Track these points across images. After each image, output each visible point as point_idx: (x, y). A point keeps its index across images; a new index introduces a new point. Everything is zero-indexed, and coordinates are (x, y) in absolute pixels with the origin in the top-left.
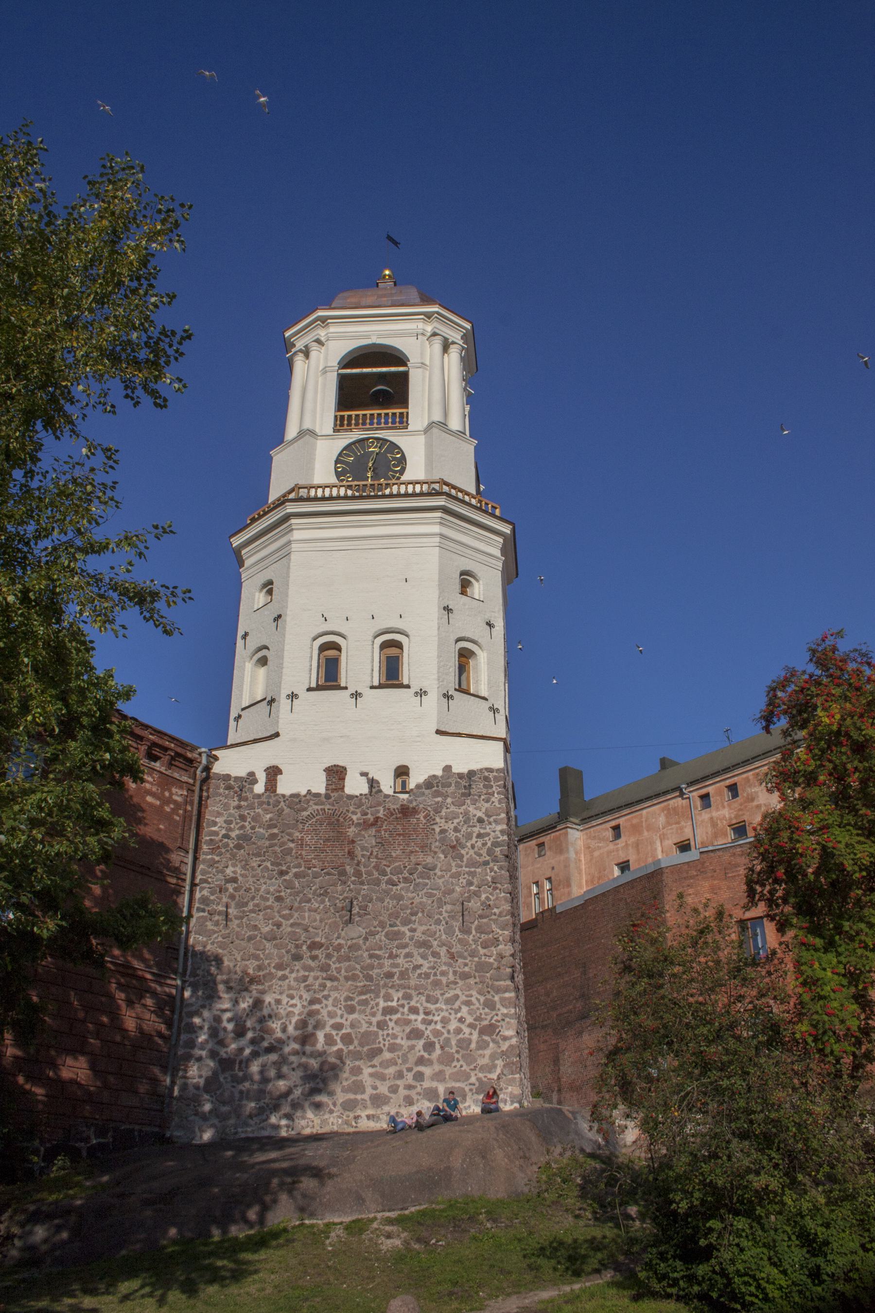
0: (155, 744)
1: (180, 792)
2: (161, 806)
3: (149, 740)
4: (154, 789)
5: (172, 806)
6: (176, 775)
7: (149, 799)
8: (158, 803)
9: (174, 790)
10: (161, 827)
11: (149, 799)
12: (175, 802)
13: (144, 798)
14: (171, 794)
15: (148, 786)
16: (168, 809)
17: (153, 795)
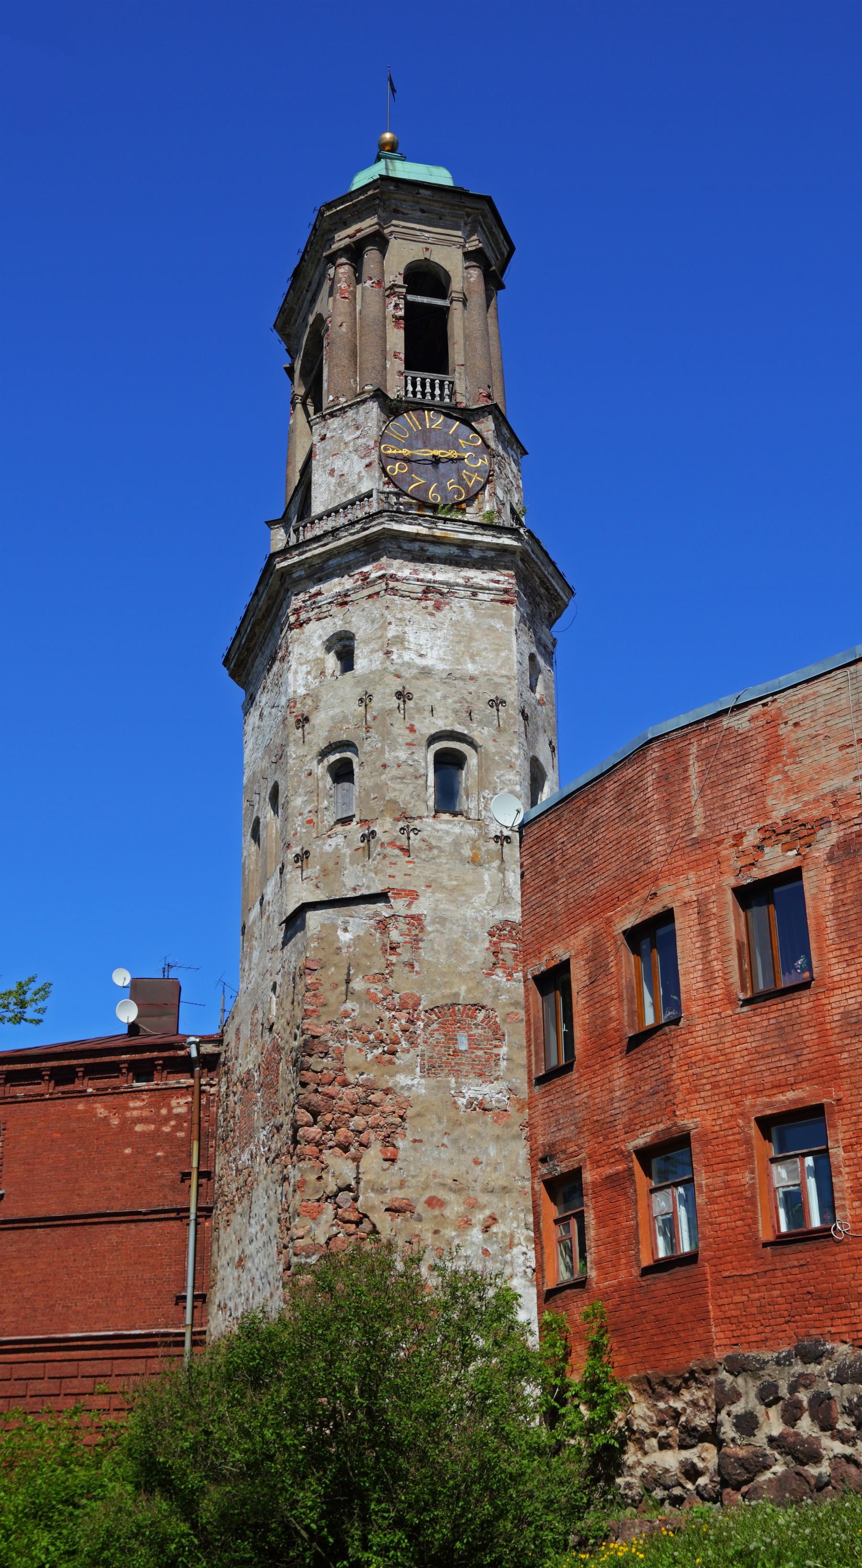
1: (182, 1101)
2: (158, 1130)
3: (124, 1062)
4: (146, 1113)
5: (173, 1123)
6: (172, 1083)
7: (139, 1128)
8: (152, 1127)
9: (174, 1102)
10: (159, 1154)
11: (139, 1128)
12: (178, 1116)
13: (132, 1129)
14: (170, 1109)
15: (135, 1113)
16: (167, 1129)
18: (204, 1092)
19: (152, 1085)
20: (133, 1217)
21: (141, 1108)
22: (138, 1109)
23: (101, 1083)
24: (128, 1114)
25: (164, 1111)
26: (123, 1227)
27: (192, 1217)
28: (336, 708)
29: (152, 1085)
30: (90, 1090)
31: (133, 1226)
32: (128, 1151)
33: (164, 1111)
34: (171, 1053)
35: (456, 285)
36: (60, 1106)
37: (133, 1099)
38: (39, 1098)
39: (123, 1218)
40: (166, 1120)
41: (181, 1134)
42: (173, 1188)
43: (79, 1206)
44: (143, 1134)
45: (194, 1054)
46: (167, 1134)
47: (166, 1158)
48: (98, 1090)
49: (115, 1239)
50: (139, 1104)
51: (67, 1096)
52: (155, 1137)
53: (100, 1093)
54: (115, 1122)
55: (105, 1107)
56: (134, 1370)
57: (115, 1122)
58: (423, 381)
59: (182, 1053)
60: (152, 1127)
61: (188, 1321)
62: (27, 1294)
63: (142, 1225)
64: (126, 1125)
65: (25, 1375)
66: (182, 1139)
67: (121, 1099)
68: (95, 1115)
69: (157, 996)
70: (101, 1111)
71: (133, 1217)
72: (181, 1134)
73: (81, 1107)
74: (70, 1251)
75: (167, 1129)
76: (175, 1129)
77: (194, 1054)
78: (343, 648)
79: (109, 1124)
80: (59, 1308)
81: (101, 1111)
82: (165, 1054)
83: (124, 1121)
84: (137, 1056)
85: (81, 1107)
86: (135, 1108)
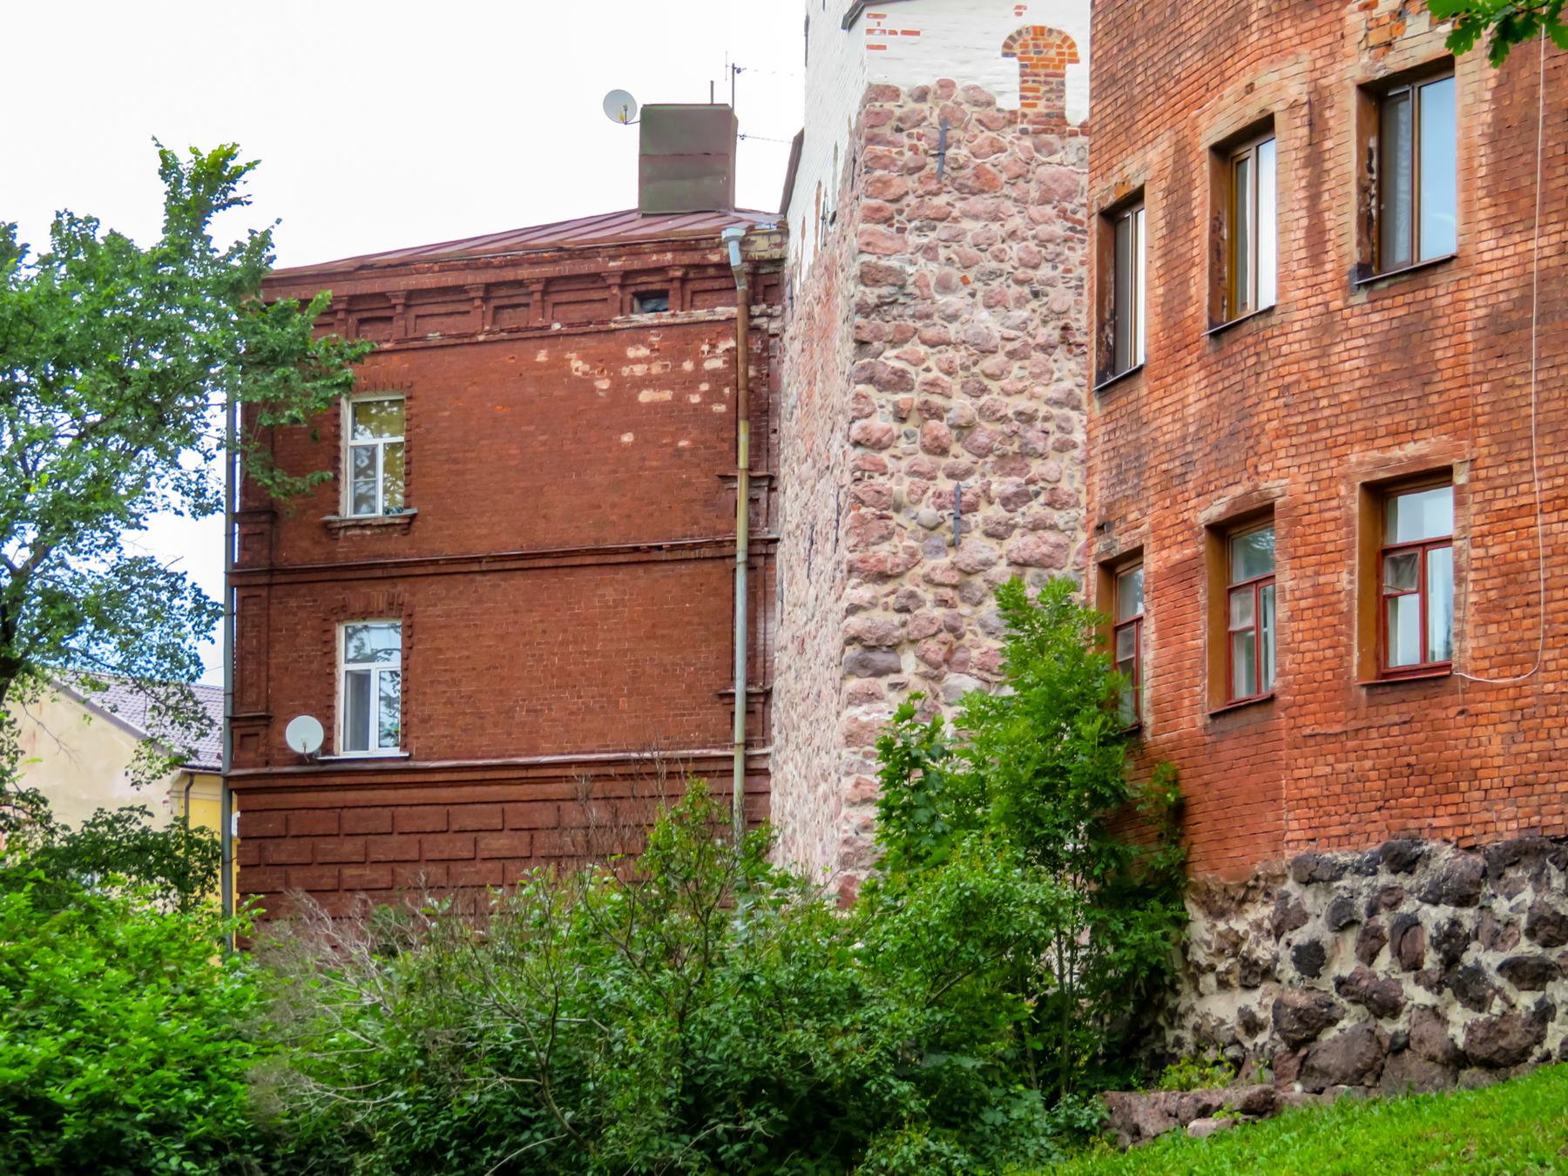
2: (678, 398)
3: (612, 273)
4: (656, 369)
5: (704, 387)
6: (701, 314)
7: (645, 396)
8: (667, 395)
10: (683, 443)
11: (645, 396)
12: (714, 375)
13: (633, 399)
15: (639, 370)
16: (695, 399)
18: (757, 329)
19: (666, 318)
22: (641, 361)
23: (576, 314)
24: (626, 371)
25: (688, 366)
26: (622, 574)
27: (741, 557)
29: (666, 318)
30: (556, 326)
31: (640, 571)
32: (627, 438)
33: (688, 366)
34: (695, 257)
36: (506, 357)
38: (464, 341)
40: (691, 382)
41: (720, 408)
43: (547, 536)
44: (652, 406)
46: (695, 407)
47: (693, 450)
48: (571, 325)
50: (644, 352)
51: (518, 335)
53: (576, 332)
54: (603, 384)
55: (584, 359)
57: (603, 384)
60: (667, 395)
61: (739, 737)
62: (466, 688)
63: (657, 571)
64: (624, 390)
65: (470, 824)
66: (721, 416)
67: (610, 344)
68: (568, 373)
71: (641, 557)
72: (720, 408)
73: (542, 357)
74: (536, 616)
76: (709, 398)
77: (735, 260)
79: (593, 390)
80: (521, 715)
81: (578, 366)
83: (618, 383)
85: (542, 357)
86: (638, 361)
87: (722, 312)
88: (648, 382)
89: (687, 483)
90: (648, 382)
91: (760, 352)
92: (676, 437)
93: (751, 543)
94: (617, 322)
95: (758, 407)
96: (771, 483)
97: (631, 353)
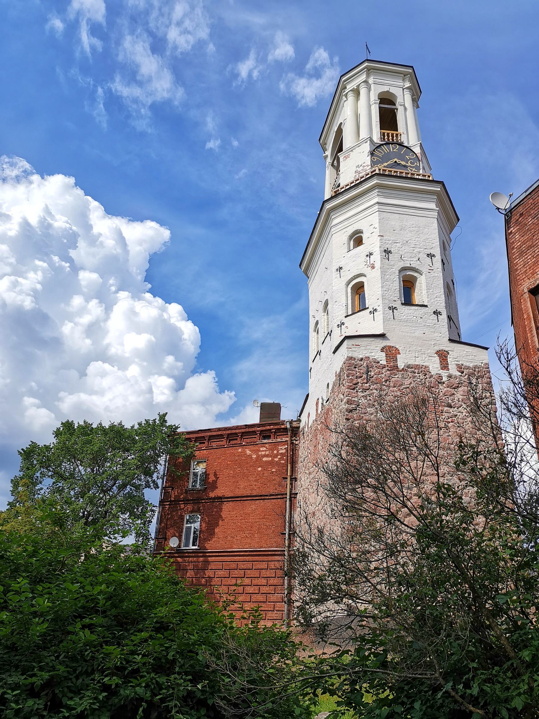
0: (262, 431)
5: (279, 457)
6: (279, 440)
7: (265, 459)
11: (265, 459)
15: (263, 453)
16: (276, 459)
17: (267, 456)
19: (270, 441)
20: (262, 497)
21: (266, 451)
23: (248, 440)
24: (260, 453)
25: (275, 452)
27: (288, 497)
28: (354, 262)
29: (270, 441)
31: (262, 501)
32: (260, 469)
33: (275, 452)
34: (278, 427)
35: (399, 100)
37: (262, 447)
39: (257, 498)
40: (276, 456)
42: (280, 485)
43: (238, 493)
44: (266, 462)
45: (288, 426)
48: (247, 443)
49: (254, 507)
50: (265, 449)
51: (234, 446)
52: (271, 463)
56: (262, 567)
58: (388, 134)
59: (283, 427)
61: (287, 545)
64: (259, 458)
65: (214, 567)
67: (256, 448)
68: (246, 454)
69: (270, 411)
70: (248, 452)
71: (262, 497)
73: (240, 450)
74: (235, 513)
75: (276, 459)
77: (288, 426)
78: (357, 239)
79: (252, 458)
80: (229, 538)
81: (248, 452)
82: (276, 427)
83: (258, 456)
84: (264, 428)
85: (240, 450)
86: (263, 451)
87: (284, 439)
88: (266, 456)
89: (274, 480)
90: (266, 456)
91: (293, 449)
92: (272, 468)
93: (291, 494)
94: (259, 442)
95: (292, 459)
96: (296, 479)
97: (261, 449)
